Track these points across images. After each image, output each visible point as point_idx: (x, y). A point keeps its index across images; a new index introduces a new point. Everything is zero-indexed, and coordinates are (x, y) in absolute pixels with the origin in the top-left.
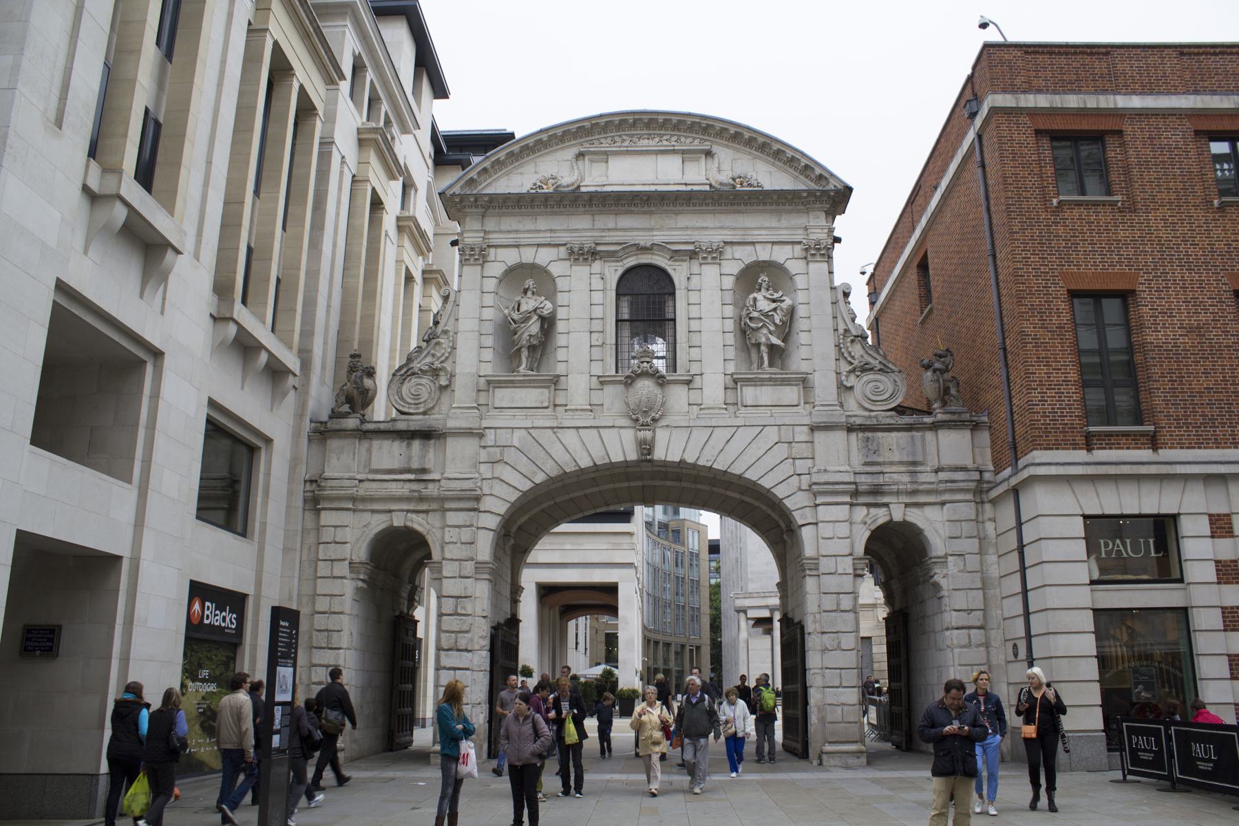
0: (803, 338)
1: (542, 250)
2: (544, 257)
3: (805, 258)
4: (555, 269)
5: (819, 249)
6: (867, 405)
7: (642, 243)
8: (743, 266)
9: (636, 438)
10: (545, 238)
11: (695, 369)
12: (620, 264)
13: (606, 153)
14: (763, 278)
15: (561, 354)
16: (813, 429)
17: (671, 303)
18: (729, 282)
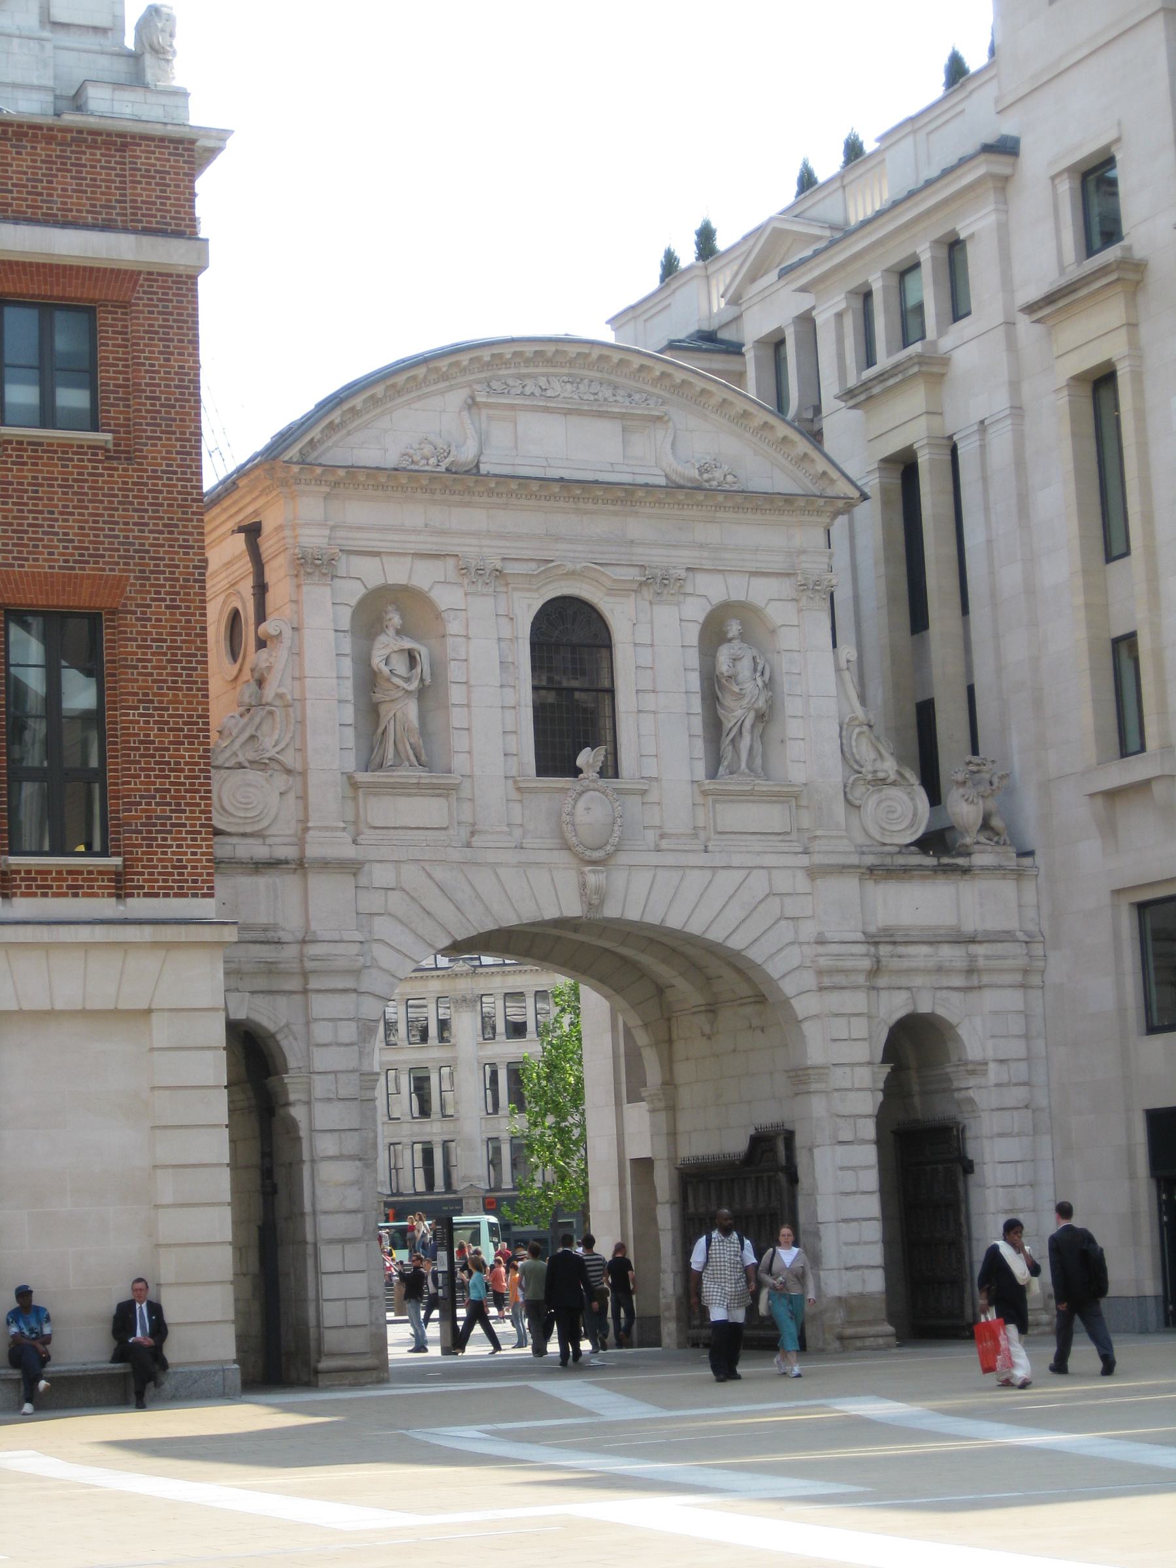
0: (794, 728)
1: (422, 566)
2: (423, 576)
3: (796, 600)
4: (445, 598)
5: (818, 591)
6: (878, 837)
7: (570, 566)
8: (709, 608)
9: (583, 885)
10: (428, 543)
11: (651, 769)
12: (536, 595)
13: (512, 407)
14: (734, 628)
15: (459, 742)
16: (814, 872)
17: (605, 664)
18: (693, 635)
